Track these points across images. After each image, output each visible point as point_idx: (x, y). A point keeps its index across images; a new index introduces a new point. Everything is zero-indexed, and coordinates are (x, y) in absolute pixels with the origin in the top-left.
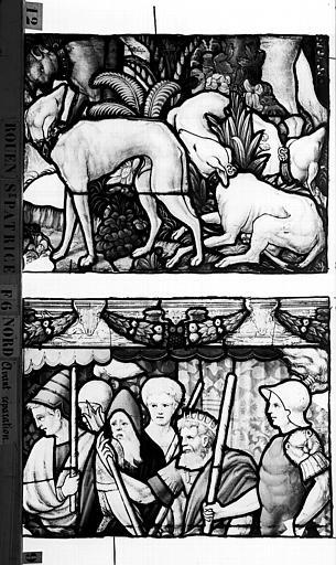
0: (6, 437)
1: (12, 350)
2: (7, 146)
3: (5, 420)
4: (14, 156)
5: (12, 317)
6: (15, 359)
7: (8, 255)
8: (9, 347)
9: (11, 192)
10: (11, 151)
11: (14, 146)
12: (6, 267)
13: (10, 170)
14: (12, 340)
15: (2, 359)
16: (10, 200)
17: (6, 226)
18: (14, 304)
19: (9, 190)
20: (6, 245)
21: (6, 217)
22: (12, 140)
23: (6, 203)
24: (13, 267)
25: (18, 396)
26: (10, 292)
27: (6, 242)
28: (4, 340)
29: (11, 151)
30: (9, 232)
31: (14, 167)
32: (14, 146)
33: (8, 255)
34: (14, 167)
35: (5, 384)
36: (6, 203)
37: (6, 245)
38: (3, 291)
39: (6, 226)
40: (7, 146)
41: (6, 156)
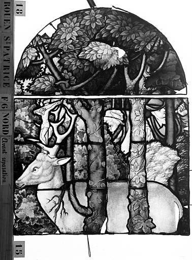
0: (4, 181)
1: (8, 131)
2: (5, 14)
4: (9, 20)
5: (8, 112)
6: (10, 136)
8: (6, 129)
9: (7, 41)
10: (7, 17)
11: (9, 14)
12: (4, 84)
13: (6, 29)
14: (8, 126)
15: (2, 136)
17: (4, 60)
18: (10, 100)
20: (7, 71)
21: (4, 55)
23: (4, 47)
24: (9, 84)
25: (12, 180)
26: (7, 98)
27: (5, 69)
28: (3, 126)
29: (7, 17)
30: (6, 64)
31: (10, 26)
32: (9, 14)
34: (10, 26)
35: (4, 151)
36: (4, 47)
37: (7, 71)
38: (2, 98)
39: (4, 60)
40: (5, 14)
41: (5, 20)
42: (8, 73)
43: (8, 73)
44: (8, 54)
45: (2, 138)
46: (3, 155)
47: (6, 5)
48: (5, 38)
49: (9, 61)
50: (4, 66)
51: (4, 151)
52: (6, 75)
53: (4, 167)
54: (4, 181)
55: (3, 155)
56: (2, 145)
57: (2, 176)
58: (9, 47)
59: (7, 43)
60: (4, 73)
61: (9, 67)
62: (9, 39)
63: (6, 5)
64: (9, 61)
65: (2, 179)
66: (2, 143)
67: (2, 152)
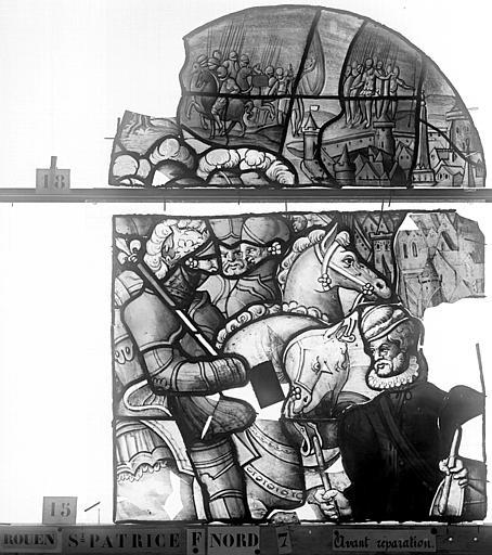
12: (172, 545)
17: (121, 546)
20: (144, 541)
24: (172, 536)
27: (140, 543)
37: (144, 541)
39: (121, 546)
42: (149, 536)
43: (149, 536)
45: (334, 549)
49: (121, 536)
50: (134, 546)
51: (364, 544)
54: (427, 544)
60: (149, 545)
61: (135, 536)
66: (346, 549)
67: (365, 549)
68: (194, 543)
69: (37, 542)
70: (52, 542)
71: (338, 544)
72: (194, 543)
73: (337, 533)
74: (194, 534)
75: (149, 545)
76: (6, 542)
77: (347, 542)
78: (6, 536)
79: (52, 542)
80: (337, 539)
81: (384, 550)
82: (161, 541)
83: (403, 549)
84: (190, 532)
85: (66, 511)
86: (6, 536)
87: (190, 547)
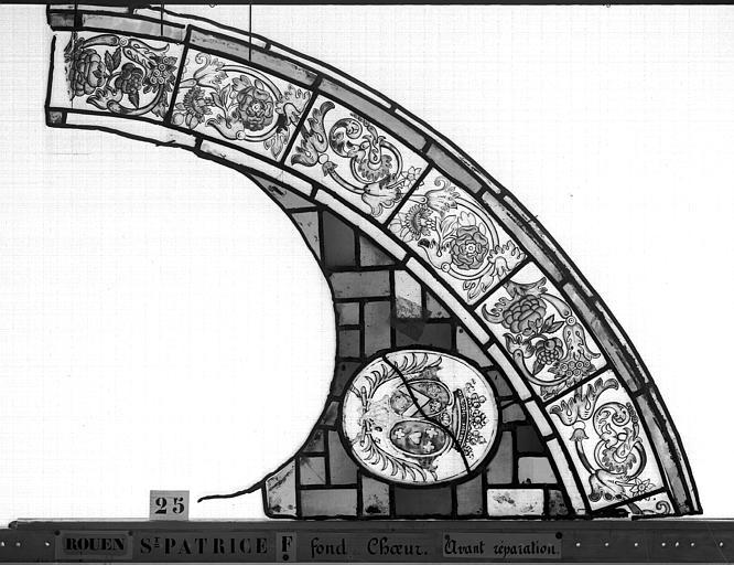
3: (527, 551)
7: (242, 548)
9: (152, 546)
12: (259, 551)
16: (162, 545)
17: (201, 551)
19: (150, 548)
21: (188, 552)
22: (74, 541)
23: (167, 551)
24: (259, 540)
27: (222, 549)
30: (209, 547)
31: (118, 541)
33: (242, 548)
34: (118, 541)
36: (167, 551)
39: (201, 551)
42: (233, 540)
43: (233, 540)
44: (185, 543)
45: (445, 554)
46: (489, 552)
47: (75, 547)
48: (144, 549)
50: (216, 551)
51: (479, 549)
52: (237, 544)
53: (518, 550)
55: (489, 552)
56: (464, 555)
57: (540, 556)
58: (167, 540)
59: (157, 546)
60: (233, 551)
61: (216, 540)
62: (146, 542)
63: (75, 547)
64: (201, 540)
65: (546, 555)
66: (458, 555)
67: (479, 555)
68: (284, 549)
69: (104, 548)
70: (121, 547)
71: (449, 550)
72: (284, 549)
73: (447, 537)
74: (285, 538)
75: (233, 551)
76: (69, 547)
77: (460, 548)
78: (69, 540)
79: (121, 547)
80: (448, 545)
81: (501, 556)
82: (246, 546)
83: (524, 556)
84: (279, 537)
85: (178, 507)
86: (69, 540)
87: (279, 553)
